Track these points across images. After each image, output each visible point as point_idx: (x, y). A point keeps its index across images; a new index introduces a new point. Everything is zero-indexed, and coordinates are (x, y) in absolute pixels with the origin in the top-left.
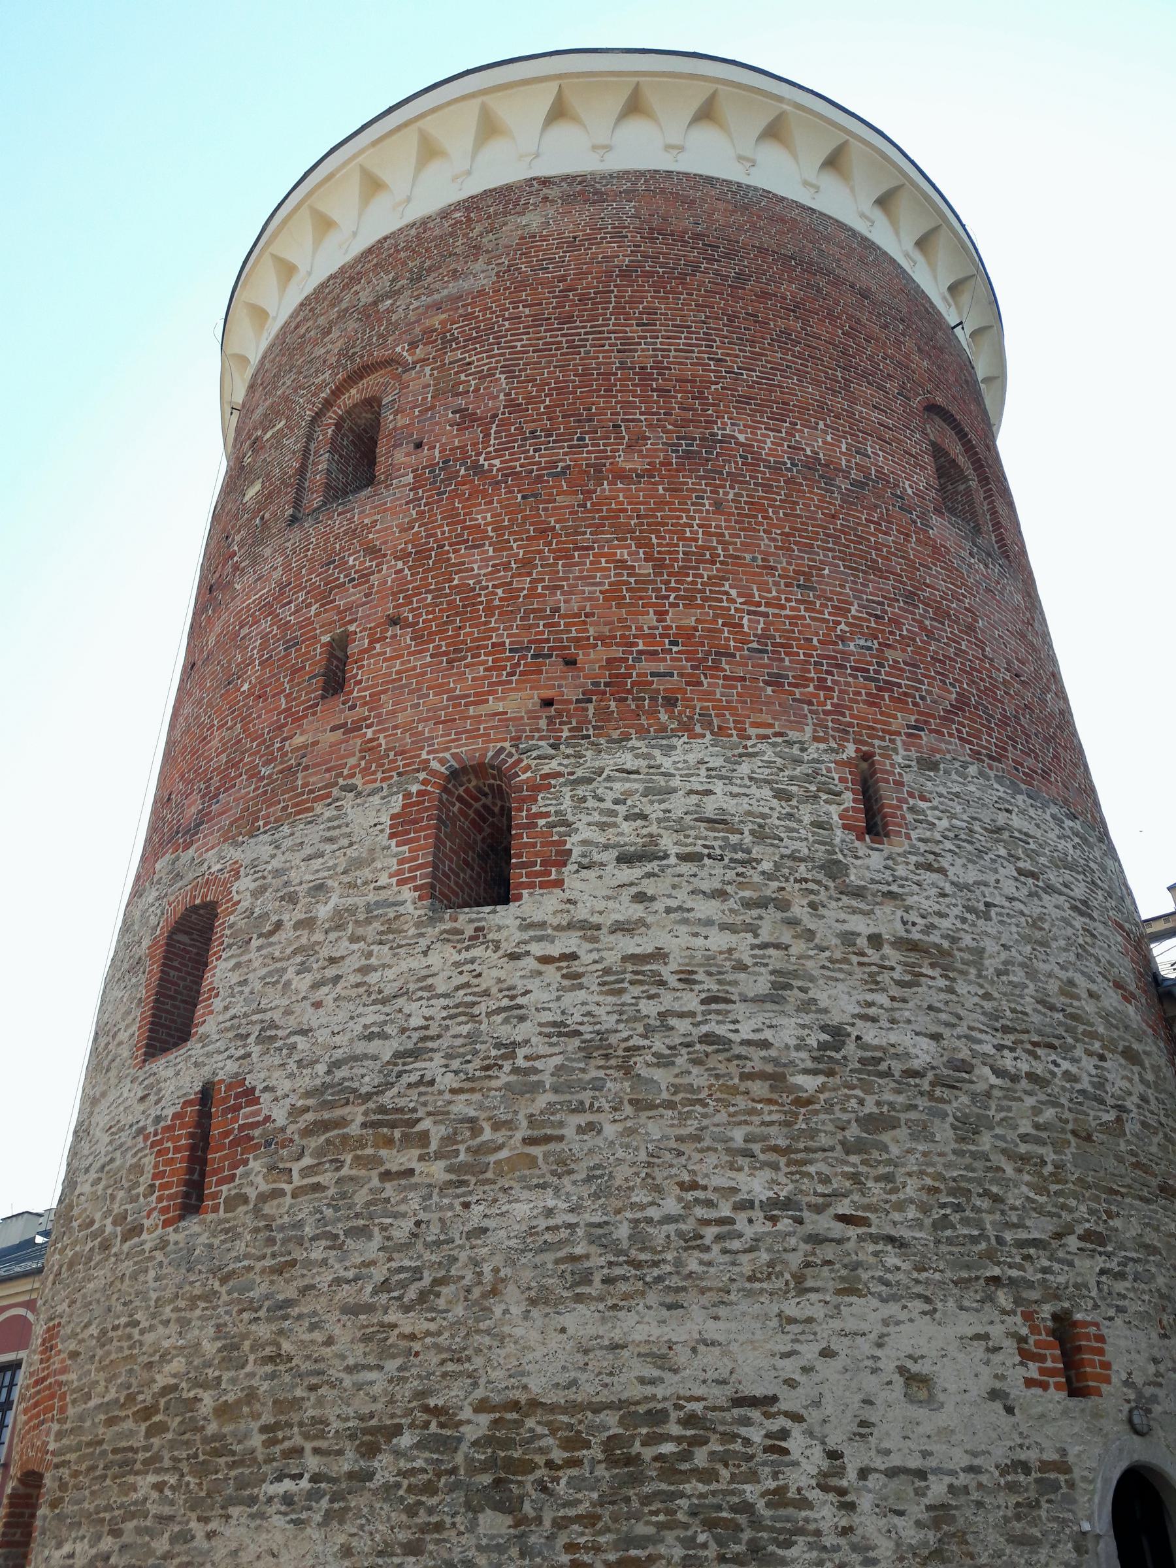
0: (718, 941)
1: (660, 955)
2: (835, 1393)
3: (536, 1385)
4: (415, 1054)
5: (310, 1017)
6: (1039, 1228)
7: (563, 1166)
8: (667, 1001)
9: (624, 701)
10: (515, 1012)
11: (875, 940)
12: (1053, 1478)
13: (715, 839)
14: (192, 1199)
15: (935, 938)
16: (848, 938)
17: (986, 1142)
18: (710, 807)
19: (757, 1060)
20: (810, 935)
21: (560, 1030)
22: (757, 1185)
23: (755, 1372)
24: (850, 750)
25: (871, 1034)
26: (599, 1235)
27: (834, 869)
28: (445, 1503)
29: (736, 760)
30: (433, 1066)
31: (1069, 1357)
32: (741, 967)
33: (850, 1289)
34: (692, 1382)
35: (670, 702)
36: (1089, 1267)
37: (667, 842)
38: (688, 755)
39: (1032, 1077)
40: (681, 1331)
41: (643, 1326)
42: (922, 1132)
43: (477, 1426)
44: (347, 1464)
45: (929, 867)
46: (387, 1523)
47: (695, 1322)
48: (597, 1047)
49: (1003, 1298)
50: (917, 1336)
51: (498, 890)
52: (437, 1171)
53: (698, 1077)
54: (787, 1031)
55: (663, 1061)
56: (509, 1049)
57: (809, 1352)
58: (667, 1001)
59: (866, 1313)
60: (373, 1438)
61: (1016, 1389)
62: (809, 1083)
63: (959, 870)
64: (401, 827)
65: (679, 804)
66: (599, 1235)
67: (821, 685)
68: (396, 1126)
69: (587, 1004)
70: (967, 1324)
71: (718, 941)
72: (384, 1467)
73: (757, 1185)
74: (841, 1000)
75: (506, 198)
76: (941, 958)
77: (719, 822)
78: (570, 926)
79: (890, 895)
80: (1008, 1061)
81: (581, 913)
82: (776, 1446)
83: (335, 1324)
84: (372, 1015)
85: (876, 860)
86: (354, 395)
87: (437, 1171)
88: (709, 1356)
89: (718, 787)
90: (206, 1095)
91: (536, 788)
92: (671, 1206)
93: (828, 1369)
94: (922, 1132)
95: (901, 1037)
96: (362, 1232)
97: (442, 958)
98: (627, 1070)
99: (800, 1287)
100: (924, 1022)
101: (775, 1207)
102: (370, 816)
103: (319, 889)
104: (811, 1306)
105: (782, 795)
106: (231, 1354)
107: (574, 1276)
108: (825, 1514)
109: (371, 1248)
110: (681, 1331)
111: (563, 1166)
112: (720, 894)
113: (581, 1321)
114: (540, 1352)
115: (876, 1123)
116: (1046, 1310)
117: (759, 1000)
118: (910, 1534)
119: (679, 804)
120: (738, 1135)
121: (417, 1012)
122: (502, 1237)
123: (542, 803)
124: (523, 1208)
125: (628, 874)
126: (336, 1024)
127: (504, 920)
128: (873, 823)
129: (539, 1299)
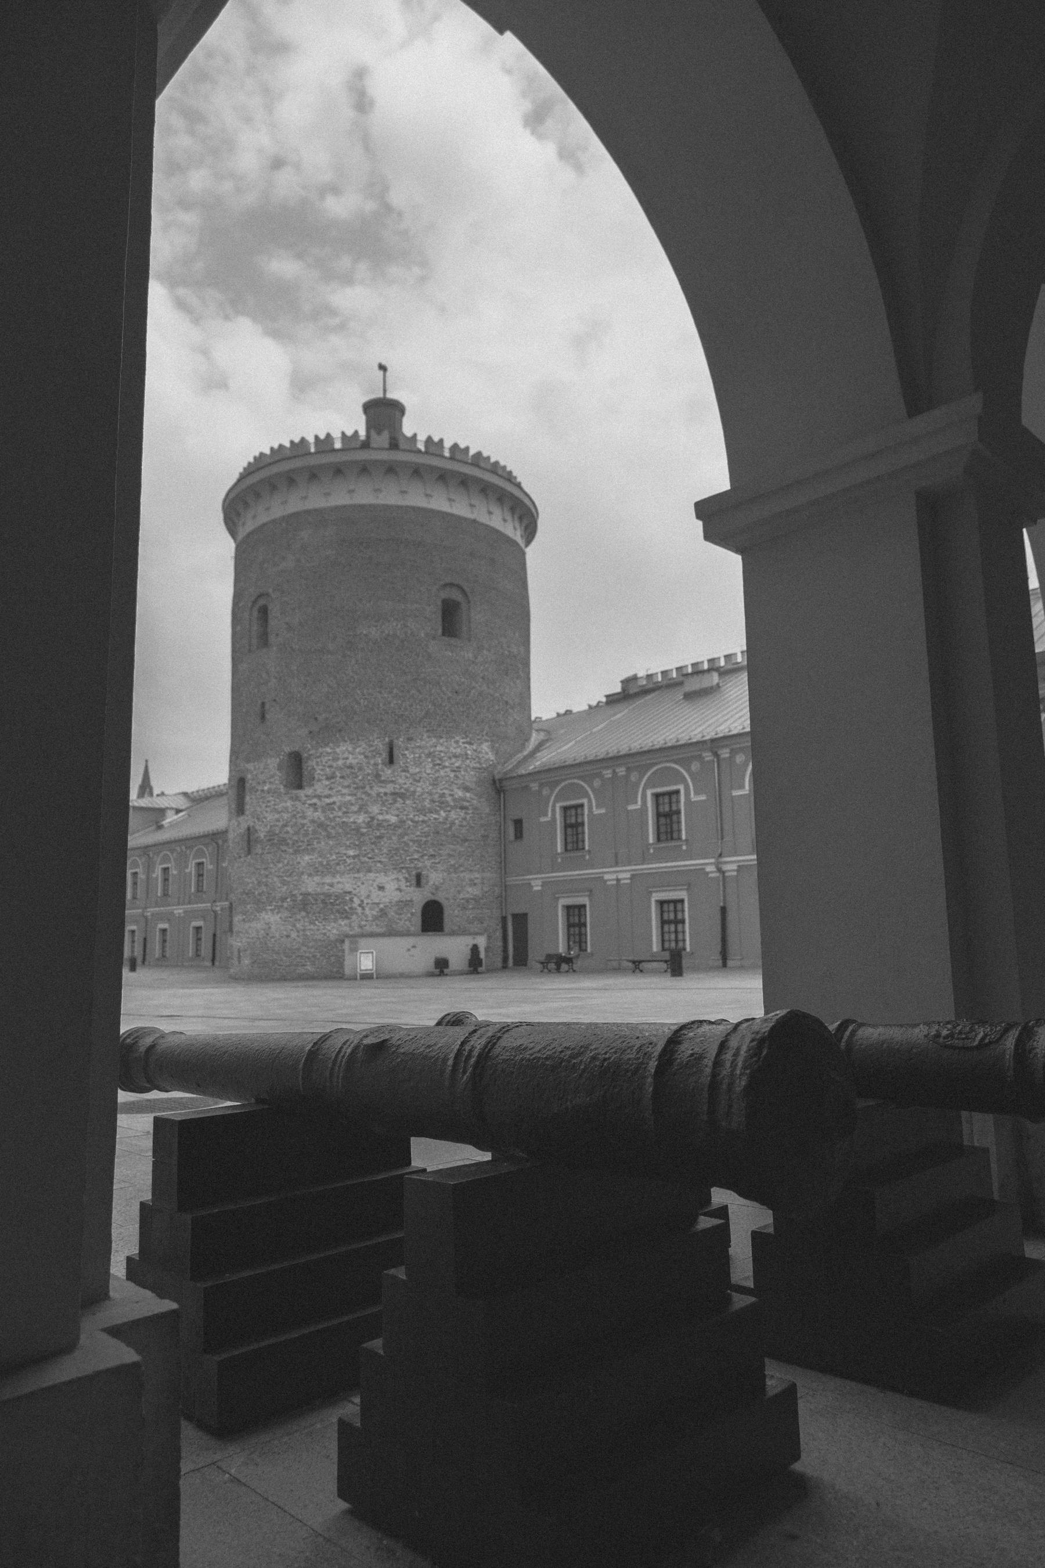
0: (349, 798)
1: (334, 803)
2: (363, 891)
3: (310, 890)
4: (285, 825)
5: (267, 815)
6: (416, 856)
7: (313, 850)
8: (335, 814)
9: (328, 733)
10: (304, 817)
11: (386, 794)
12: (409, 903)
13: (348, 771)
14: (249, 852)
15: (403, 790)
16: (378, 795)
17: (406, 838)
18: (348, 762)
19: (353, 826)
20: (369, 795)
21: (313, 821)
22: (351, 853)
23: (348, 887)
24: (387, 739)
25: (380, 817)
26: (321, 863)
27: (378, 776)
28: (295, 910)
29: (354, 749)
30: (289, 829)
31: (419, 880)
32: (352, 804)
33: (370, 871)
34: (337, 889)
35: (340, 731)
36: (428, 863)
37: (338, 774)
38: (343, 748)
39: (423, 821)
40: (335, 881)
41: (328, 880)
42: (390, 838)
43: (300, 898)
44: (280, 904)
45: (404, 771)
46: (286, 914)
47: (338, 878)
48: (321, 825)
49: (404, 871)
50: (382, 879)
51: (300, 787)
52: (291, 850)
53: (340, 831)
54: (361, 819)
55: (333, 828)
56: (303, 825)
57: (359, 884)
58: (335, 814)
59: (372, 875)
60: (283, 900)
61: (403, 887)
62: (365, 830)
63: (414, 770)
64: (280, 768)
65: (340, 763)
66: (321, 863)
67: (382, 720)
68: (283, 841)
69: (318, 815)
70: (393, 877)
71: (349, 798)
72: (285, 905)
73: (351, 853)
74: (375, 809)
75: (295, 519)
76: (402, 796)
77: (351, 767)
78: (315, 796)
79: (392, 782)
80: (417, 818)
81: (318, 792)
82: (351, 900)
83: (275, 879)
84: (277, 816)
85: (389, 772)
86: (257, 607)
87: (291, 850)
88: (340, 886)
89: (351, 756)
90: (249, 829)
91: (308, 758)
92: (334, 857)
93: (363, 887)
94: (390, 838)
95: (388, 817)
96: (279, 862)
97: (289, 804)
98: (326, 830)
99: (358, 871)
100: (396, 812)
101: (354, 857)
102: (273, 763)
103: (264, 782)
104: (361, 875)
105: (366, 757)
106: (259, 883)
107: (317, 870)
108: (359, 910)
109: (280, 865)
110: (335, 881)
111: (313, 850)
112: (349, 787)
113: (317, 879)
114: (311, 885)
115: (380, 837)
116: (414, 873)
117: (356, 812)
118: (375, 913)
119: (340, 763)
120: (348, 843)
121: (286, 816)
122: (303, 864)
123: (310, 763)
124: (307, 858)
125: (327, 783)
126: (270, 817)
127: (301, 793)
128: (391, 760)
129: (310, 875)
